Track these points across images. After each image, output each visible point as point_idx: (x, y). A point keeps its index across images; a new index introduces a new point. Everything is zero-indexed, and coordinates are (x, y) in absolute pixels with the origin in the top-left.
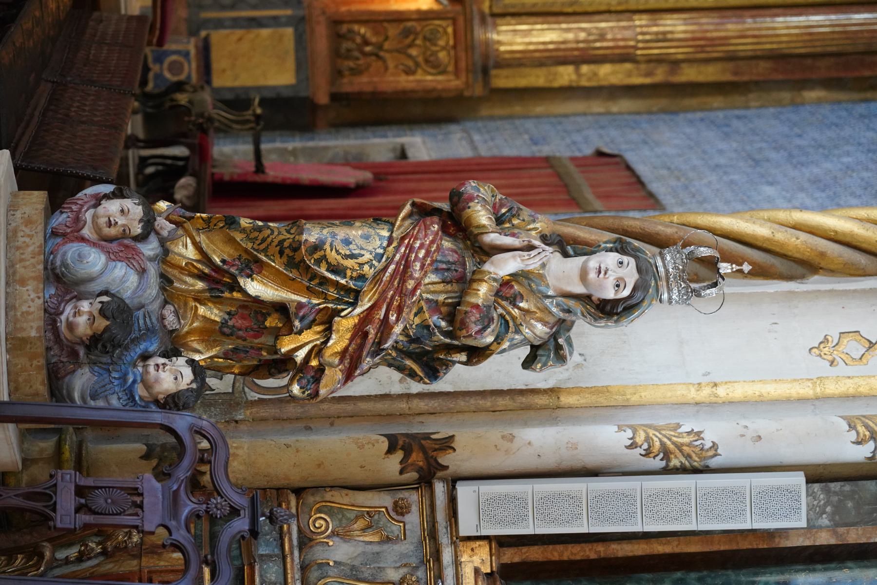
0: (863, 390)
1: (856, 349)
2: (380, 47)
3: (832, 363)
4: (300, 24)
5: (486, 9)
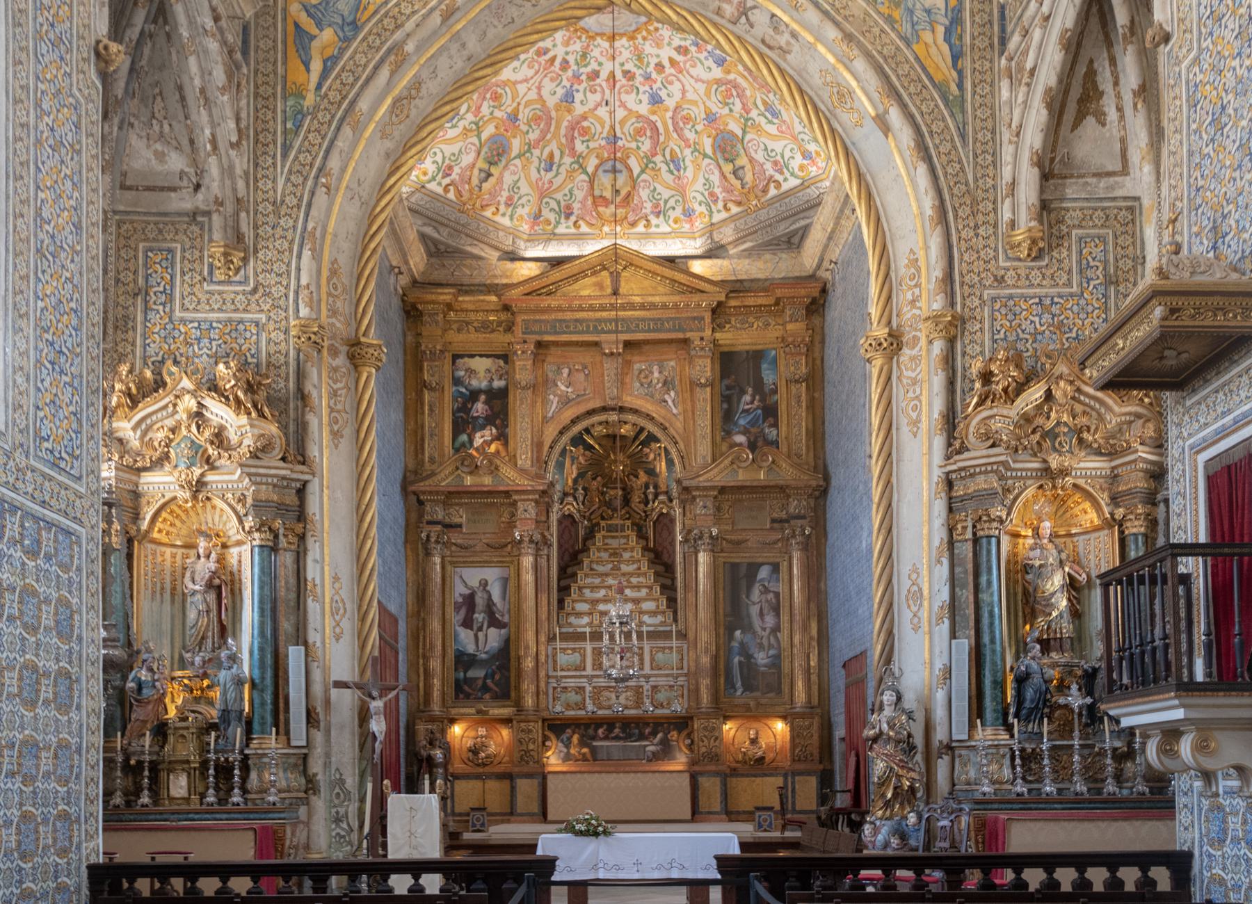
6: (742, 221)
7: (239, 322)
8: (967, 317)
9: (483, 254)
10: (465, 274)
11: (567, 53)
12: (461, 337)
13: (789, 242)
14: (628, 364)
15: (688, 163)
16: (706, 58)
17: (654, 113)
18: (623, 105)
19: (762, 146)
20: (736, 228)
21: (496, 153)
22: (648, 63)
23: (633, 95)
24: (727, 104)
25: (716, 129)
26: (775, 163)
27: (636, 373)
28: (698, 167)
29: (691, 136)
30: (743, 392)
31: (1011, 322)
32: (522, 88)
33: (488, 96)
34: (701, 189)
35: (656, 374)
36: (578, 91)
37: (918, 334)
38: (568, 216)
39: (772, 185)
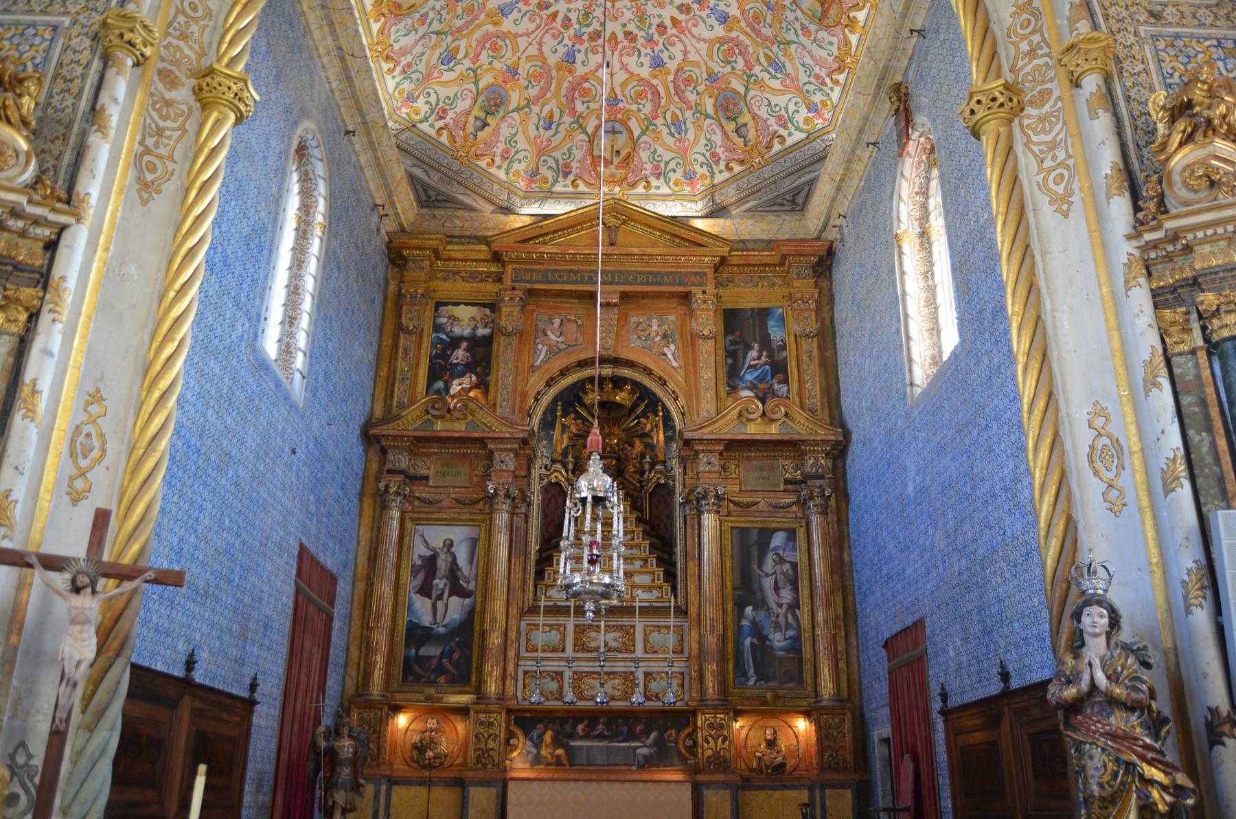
0: (1144, 487)
1: (1113, 494)
2: (833, 749)
3: (1124, 505)
4: (824, 786)
5: (813, 700)
6: (745, 180)
7: (29, 26)
8: (1121, 55)
9: (475, 205)
10: (458, 223)
11: (569, 10)
12: (448, 285)
13: (793, 202)
14: (624, 319)
15: (689, 125)
17: (655, 77)
18: (624, 67)
19: (766, 102)
20: (739, 188)
21: (494, 104)
22: (650, 24)
23: (635, 58)
24: (730, 63)
25: (718, 89)
26: (780, 118)
28: (699, 128)
29: (692, 97)
30: (749, 348)
31: (1185, 65)
32: (523, 42)
33: (488, 45)
34: (703, 150)
36: (579, 51)
37: (1048, 85)
38: (566, 175)
39: (776, 140)
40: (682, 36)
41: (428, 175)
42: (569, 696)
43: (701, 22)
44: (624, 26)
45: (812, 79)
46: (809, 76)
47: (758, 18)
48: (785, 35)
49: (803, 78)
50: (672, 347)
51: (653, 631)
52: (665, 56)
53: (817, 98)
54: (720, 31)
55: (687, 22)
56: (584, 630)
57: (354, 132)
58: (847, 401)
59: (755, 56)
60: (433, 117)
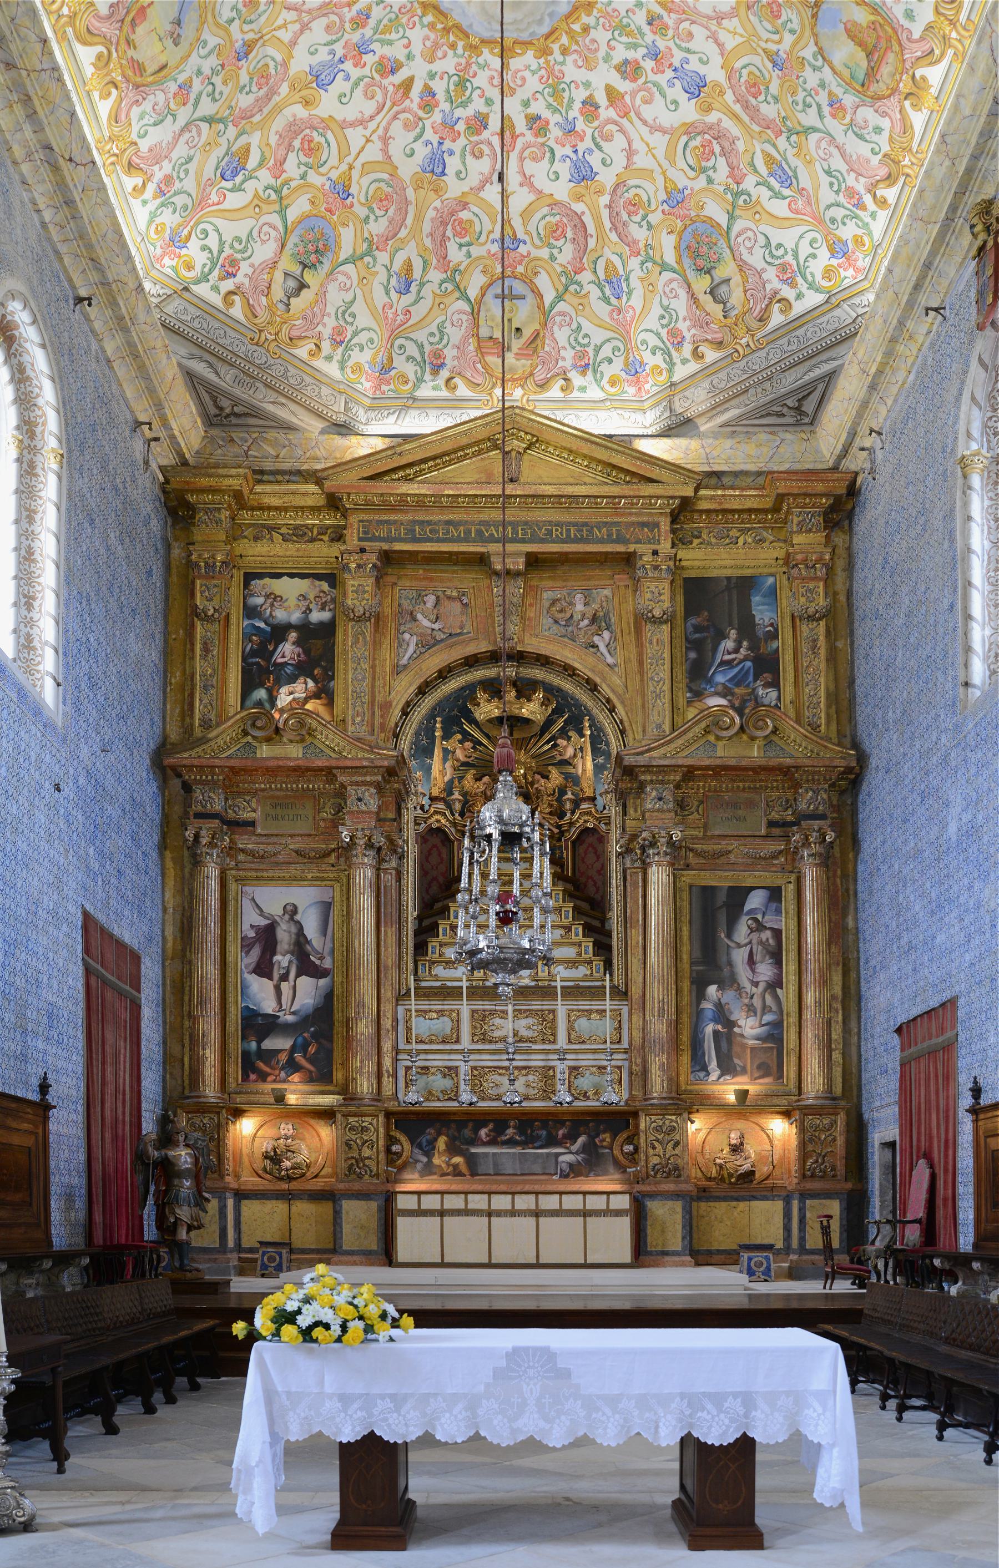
16: (671, 84)
18: (527, 181)
22: (571, 101)
23: (545, 163)
27: (547, 604)
35: (580, 607)
40: (624, 122)
41: (217, 373)
42: (466, 1096)
43: (657, 94)
44: (526, 104)
45: (842, 199)
46: (837, 192)
47: (755, 87)
48: (801, 116)
49: (827, 196)
50: (606, 635)
51: (578, 1017)
52: (595, 160)
53: (848, 232)
54: (689, 111)
55: (634, 94)
56: (485, 1016)
57: (89, 299)
58: (862, 713)
59: (747, 158)
60: (216, 273)
